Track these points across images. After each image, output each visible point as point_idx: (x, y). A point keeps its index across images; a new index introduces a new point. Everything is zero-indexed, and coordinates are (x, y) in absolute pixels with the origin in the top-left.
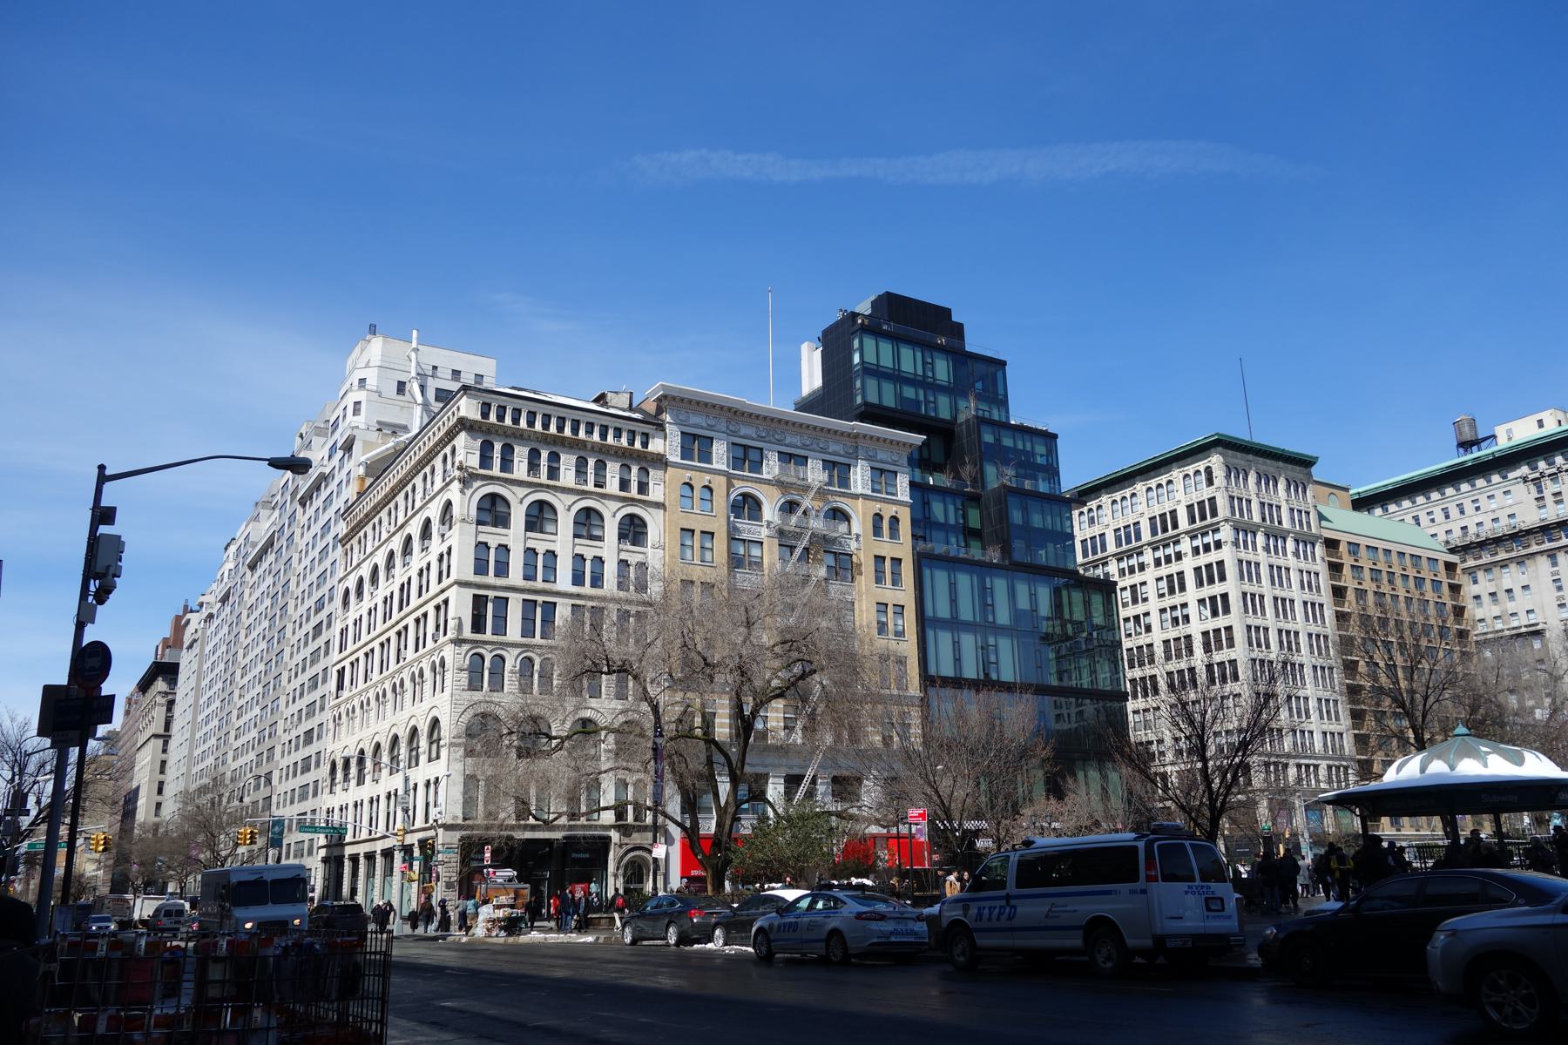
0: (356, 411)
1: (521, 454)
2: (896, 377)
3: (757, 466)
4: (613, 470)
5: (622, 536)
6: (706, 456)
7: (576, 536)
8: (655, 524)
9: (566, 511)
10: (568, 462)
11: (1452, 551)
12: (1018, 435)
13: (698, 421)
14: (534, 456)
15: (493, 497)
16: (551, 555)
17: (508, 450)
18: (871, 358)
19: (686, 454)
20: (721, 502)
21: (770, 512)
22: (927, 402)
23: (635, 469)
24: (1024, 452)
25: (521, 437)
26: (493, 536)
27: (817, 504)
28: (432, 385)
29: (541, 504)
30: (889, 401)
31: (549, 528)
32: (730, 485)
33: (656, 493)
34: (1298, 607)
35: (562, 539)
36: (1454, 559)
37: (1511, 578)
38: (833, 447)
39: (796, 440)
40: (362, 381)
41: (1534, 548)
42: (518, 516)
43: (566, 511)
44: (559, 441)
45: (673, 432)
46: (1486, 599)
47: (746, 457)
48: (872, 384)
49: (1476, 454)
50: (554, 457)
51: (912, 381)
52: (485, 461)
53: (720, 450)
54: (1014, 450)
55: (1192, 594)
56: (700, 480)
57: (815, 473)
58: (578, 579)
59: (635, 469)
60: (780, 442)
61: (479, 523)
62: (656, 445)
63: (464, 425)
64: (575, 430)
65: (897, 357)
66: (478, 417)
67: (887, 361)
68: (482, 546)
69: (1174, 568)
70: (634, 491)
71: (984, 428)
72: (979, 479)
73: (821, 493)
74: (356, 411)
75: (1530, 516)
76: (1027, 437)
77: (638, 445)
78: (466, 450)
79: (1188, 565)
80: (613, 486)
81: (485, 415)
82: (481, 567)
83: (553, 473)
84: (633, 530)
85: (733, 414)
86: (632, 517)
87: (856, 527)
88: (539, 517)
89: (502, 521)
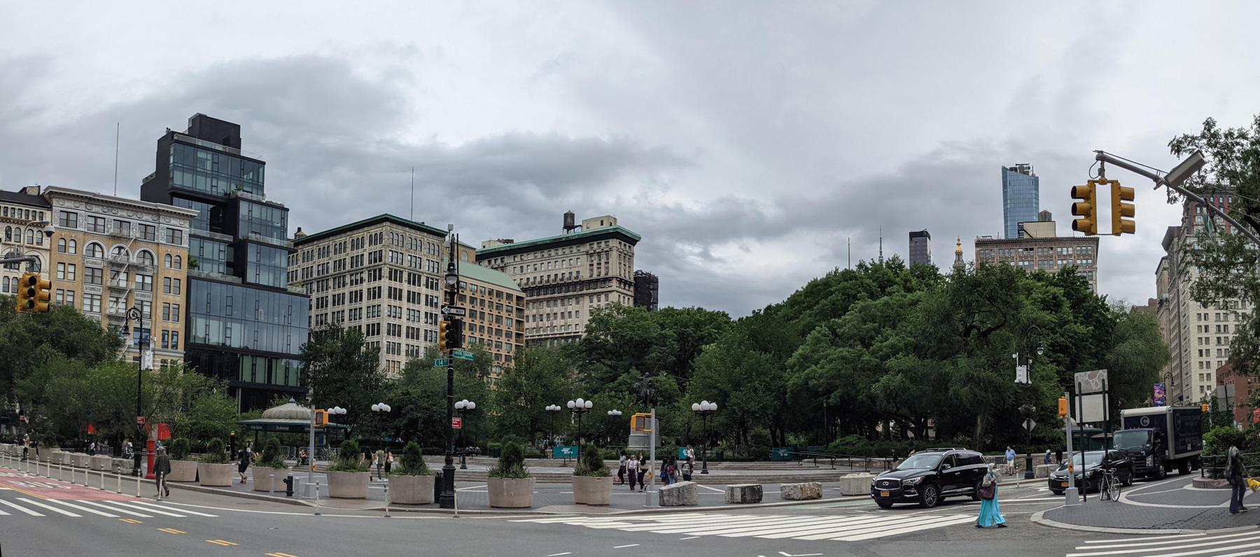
11: (524, 290)
12: (264, 209)
34: (423, 316)
36: (523, 295)
37: (572, 307)
41: (585, 291)
46: (559, 316)
49: (572, 232)
55: (365, 303)
69: (358, 288)
75: (585, 276)
79: (365, 286)
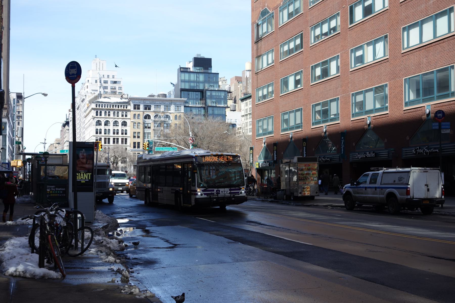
0: (87, 88)
1: (103, 112)
2: (189, 81)
3: (150, 109)
4: (120, 113)
5: (122, 125)
6: (139, 109)
7: (114, 126)
8: (128, 122)
9: (111, 121)
10: (112, 113)
12: (217, 92)
13: (137, 102)
14: (106, 112)
15: (99, 121)
16: (109, 130)
17: (101, 112)
18: (183, 78)
19: (135, 108)
20: (142, 117)
21: (152, 118)
22: (197, 86)
23: (124, 112)
24: (218, 96)
25: (103, 109)
26: (99, 127)
27: (163, 115)
28: (103, 80)
29: (107, 121)
30: (187, 87)
31: (109, 125)
32: (143, 113)
33: (129, 117)
35: (111, 127)
38: (167, 103)
39: (158, 103)
40: (88, 81)
42: (103, 124)
43: (111, 121)
44: (110, 109)
45: (132, 105)
47: (147, 107)
48: (183, 84)
50: (109, 112)
51: (194, 82)
52: (97, 115)
53: (142, 107)
54: (216, 96)
56: (137, 113)
57: (162, 108)
58: (114, 133)
59: (124, 112)
60: (155, 103)
61: (96, 125)
62: (129, 108)
63: (93, 109)
64: (113, 107)
65: (189, 77)
66: (95, 107)
67: (187, 78)
68: (97, 129)
70: (124, 117)
71: (207, 92)
72: (206, 104)
73: (163, 112)
74: (87, 88)
76: (219, 92)
77: (125, 108)
78: (93, 113)
80: (120, 116)
81: (97, 106)
82: (97, 133)
83: (109, 115)
84: (124, 124)
85: (144, 100)
86: (124, 121)
87: (171, 119)
88: (106, 123)
89: (100, 124)
